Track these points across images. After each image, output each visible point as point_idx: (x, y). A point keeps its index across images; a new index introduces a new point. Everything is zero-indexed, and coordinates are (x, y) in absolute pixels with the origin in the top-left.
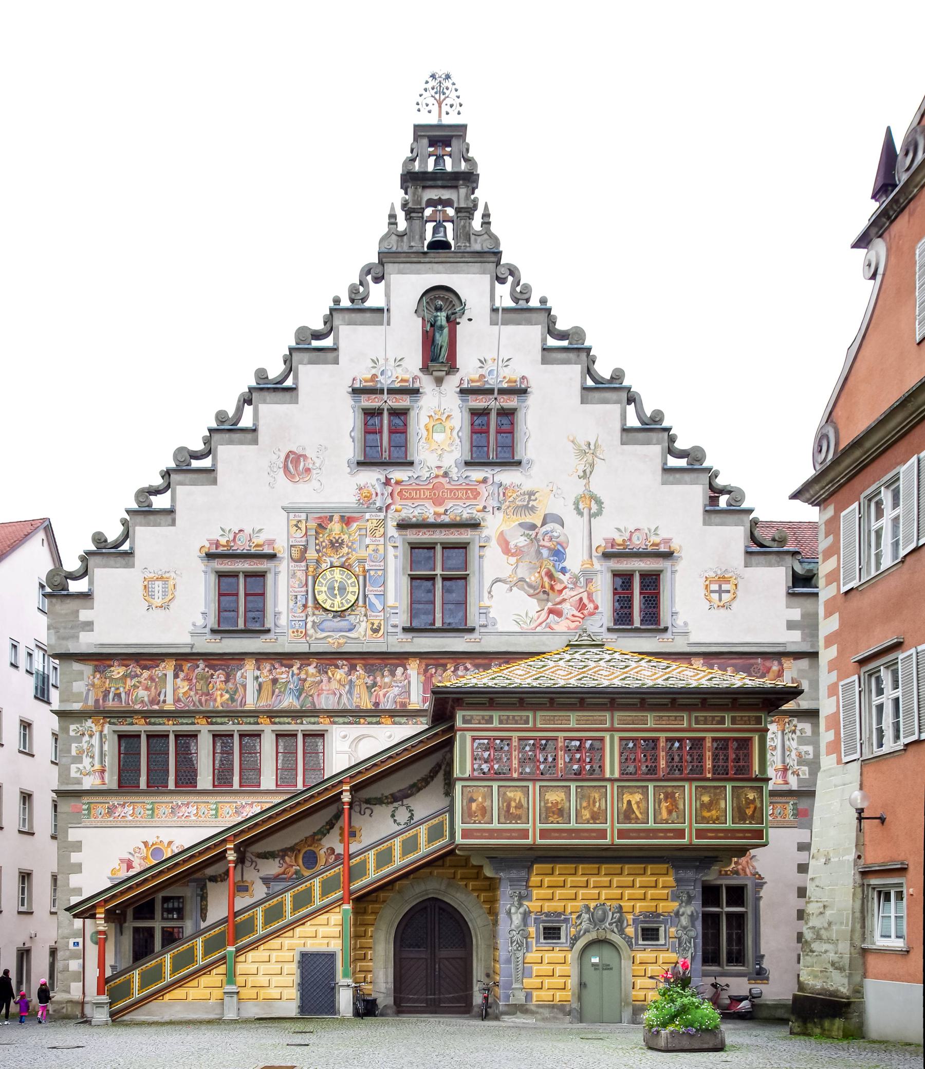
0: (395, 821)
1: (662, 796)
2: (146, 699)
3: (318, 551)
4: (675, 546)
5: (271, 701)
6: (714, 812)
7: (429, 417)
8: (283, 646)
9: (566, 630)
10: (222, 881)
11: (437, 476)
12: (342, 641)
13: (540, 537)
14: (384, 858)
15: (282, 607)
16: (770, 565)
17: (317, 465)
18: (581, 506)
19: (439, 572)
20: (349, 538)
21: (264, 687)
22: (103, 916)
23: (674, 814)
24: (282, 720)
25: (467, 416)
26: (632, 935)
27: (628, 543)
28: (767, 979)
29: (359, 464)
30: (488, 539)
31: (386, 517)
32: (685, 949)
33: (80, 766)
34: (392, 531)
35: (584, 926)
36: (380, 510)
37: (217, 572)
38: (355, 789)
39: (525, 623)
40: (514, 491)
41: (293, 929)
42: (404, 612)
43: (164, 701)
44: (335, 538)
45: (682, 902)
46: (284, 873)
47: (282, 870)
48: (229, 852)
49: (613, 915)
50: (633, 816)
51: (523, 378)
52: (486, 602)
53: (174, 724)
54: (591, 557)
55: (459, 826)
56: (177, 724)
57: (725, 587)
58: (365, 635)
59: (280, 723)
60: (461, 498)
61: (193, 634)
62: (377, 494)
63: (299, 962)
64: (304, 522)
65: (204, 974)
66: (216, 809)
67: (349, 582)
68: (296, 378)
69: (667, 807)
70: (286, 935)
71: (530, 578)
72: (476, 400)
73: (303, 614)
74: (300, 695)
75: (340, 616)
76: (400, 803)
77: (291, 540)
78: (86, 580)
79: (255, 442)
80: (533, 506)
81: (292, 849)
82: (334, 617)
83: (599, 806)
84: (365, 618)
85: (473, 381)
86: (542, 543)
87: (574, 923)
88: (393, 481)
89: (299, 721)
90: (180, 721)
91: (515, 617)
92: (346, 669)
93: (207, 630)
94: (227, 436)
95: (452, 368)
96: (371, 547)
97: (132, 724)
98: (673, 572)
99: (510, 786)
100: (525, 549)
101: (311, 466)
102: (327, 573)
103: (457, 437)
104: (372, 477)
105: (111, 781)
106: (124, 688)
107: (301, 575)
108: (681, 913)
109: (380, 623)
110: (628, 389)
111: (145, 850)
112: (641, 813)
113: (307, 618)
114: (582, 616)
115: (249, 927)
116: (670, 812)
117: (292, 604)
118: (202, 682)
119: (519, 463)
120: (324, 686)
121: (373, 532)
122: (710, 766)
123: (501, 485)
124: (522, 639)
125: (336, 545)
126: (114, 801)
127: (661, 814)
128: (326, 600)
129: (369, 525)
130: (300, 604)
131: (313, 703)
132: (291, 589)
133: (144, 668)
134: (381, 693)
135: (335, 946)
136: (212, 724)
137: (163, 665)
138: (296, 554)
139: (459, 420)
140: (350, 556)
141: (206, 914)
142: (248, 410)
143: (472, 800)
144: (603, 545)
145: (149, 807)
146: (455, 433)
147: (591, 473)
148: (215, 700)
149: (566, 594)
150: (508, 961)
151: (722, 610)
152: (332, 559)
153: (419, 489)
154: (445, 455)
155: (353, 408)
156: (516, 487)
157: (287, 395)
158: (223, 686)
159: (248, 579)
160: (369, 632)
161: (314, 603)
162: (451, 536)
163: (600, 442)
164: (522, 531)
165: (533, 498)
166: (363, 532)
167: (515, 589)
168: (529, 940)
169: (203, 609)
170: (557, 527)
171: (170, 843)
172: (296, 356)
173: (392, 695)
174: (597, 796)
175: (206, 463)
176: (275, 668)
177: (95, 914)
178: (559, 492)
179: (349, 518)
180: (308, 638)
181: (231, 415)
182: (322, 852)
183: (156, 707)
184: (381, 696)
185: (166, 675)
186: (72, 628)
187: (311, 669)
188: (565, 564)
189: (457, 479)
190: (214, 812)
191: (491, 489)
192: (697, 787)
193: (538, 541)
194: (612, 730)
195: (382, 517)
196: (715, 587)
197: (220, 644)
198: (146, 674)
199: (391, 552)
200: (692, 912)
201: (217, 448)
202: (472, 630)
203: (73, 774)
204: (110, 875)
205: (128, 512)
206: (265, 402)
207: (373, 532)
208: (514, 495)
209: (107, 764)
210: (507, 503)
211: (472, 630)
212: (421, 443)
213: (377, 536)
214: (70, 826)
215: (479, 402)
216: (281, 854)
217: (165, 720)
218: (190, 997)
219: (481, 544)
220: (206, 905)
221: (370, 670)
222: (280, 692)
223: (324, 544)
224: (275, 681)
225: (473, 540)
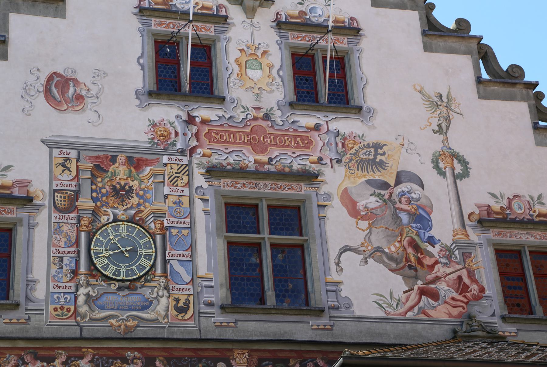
3: (95, 200)
7: (241, 51)
9: (446, 317)
11: (255, 119)
12: (131, 323)
13: (395, 197)
17: (94, 92)
18: (442, 165)
20: (140, 185)
27: (508, 212)
29: (150, 94)
30: (328, 197)
34: (199, 180)
36: (182, 152)
39: (390, 306)
40: (355, 143)
42: (221, 285)
44: (119, 184)
51: (352, 19)
54: (464, 226)
58: (166, 316)
60: (288, 146)
62: (177, 134)
64: (74, 161)
67: (142, 242)
71: (389, 248)
72: (298, 37)
75: (128, 288)
77: (54, 182)
80: (381, 161)
82: (119, 289)
84: (165, 292)
85: (292, 17)
86: (398, 205)
96: (171, 199)
100: (378, 212)
101: (84, 93)
102: (109, 228)
103: (277, 77)
109: (187, 300)
113: (77, 290)
114: (466, 300)
117: (54, 269)
121: (173, 180)
123: (338, 134)
124: (388, 327)
128: (108, 265)
129: (167, 169)
132: (53, 249)
140: (142, 207)
144: (477, 212)
146: (274, 71)
147: (448, 128)
149: (439, 270)
152: (116, 211)
154: (264, 95)
155: (141, 31)
156: (356, 139)
160: (172, 312)
161: (89, 269)
163: (453, 94)
164: (371, 190)
165: (380, 151)
166: (160, 179)
167: (371, 261)
170: (415, 187)
178: (412, 147)
179: (139, 160)
180: (79, 319)
188: (432, 233)
189: (281, 123)
191: (326, 138)
193: (394, 203)
199: (199, 206)
207: (173, 180)
208: (356, 147)
210: (348, 156)
211: (319, 312)
212: (231, 79)
213: (180, 185)
219: (321, 203)
225: (309, 197)
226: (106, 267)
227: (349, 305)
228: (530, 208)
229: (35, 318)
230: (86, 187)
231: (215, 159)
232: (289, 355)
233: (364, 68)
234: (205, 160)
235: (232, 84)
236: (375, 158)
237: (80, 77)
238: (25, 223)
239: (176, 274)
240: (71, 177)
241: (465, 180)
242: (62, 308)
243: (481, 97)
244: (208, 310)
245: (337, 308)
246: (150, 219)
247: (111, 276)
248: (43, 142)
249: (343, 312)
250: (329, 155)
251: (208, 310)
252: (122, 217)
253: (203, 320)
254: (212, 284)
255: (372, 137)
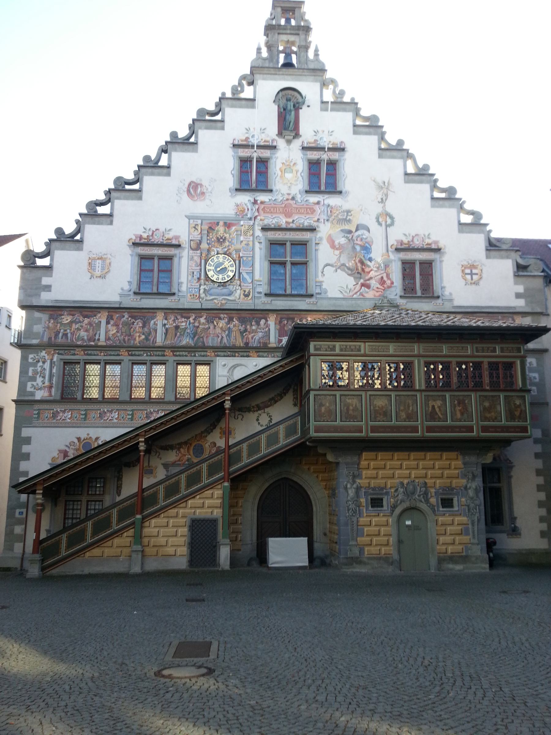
0: (259, 423)
1: (456, 402)
2: (86, 338)
3: (208, 244)
4: (441, 245)
5: (174, 340)
6: (493, 414)
7: (283, 163)
8: (184, 304)
9: (372, 297)
10: (134, 466)
11: (287, 200)
12: (223, 302)
13: (354, 238)
14: (254, 448)
15: (184, 278)
16: (502, 258)
18: (380, 220)
19: (288, 259)
21: (170, 331)
22: (41, 492)
23: (465, 415)
24: (181, 353)
25: (306, 164)
26: (435, 504)
28: (520, 534)
30: (321, 239)
31: (254, 224)
32: (472, 514)
33: (35, 383)
34: (258, 233)
35: (400, 497)
36: (250, 219)
37: (139, 255)
38: (233, 400)
39: (346, 292)
40: (337, 210)
41: (186, 501)
43: (99, 340)
45: (469, 480)
46: (179, 460)
47: (178, 458)
48: (140, 444)
49: (420, 489)
50: (437, 416)
51: (342, 142)
52: (320, 278)
53: (104, 355)
54: (388, 251)
55: (313, 424)
56: (107, 355)
57: (474, 271)
58: (240, 298)
59: (180, 356)
60: (303, 213)
61: (121, 295)
62: (248, 210)
63: (190, 526)
65: (117, 536)
66: (132, 415)
68: (197, 137)
69: (460, 410)
70: (181, 505)
73: (198, 284)
74: (194, 337)
75: (223, 286)
76: (263, 411)
78: (48, 258)
79: (169, 174)
80: (350, 219)
81: (186, 443)
82: (219, 286)
83: (412, 409)
84: (239, 287)
85: (310, 143)
86: (356, 242)
87: (393, 495)
88: (259, 202)
89: (193, 354)
90: (109, 353)
91: (340, 288)
92: (227, 320)
93: (131, 293)
94: (150, 170)
95: (297, 135)
96: (244, 243)
97: (74, 354)
98: (441, 262)
99: (348, 395)
101: (205, 191)
102: (215, 258)
104: (245, 199)
105: (55, 393)
106: (71, 330)
107: (197, 259)
108: (468, 487)
110: (407, 150)
111: (78, 444)
112: (442, 414)
115: (154, 499)
116: (462, 414)
117: (190, 277)
118: (126, 327)
119: (340, 192)
120: (211, 331)
121: (246, 233)
122: (488, 382)
124: (344, 302)
125: (221, 241)
126: (58, 408)
127: (456, 414)
129: (243, 228)
130: (195, 277)
131: (203, 342)
132: (190, 268)
133: (85, 316)
134: (250, 336)
135: (217, 513)
136: (132, 355)
137: (99, 315)
138: (193, 245)
139: (301, 166)
141: (120, 490)
142: (164, 157)
143: (321, 405)
144: (396, 244)
145: (83, 412)
147: (386, 200)
148: (135, 339)
149: (372, 274)
150: (346, 524)
151: (474, 286)
152: (218, 249)
153: (276, 208)
157: (191, 147)
158: (141, 330)
159: (161, 261)
160: (242, 296)
162: (297, 237)
164: (343, 234)
165: (349, 214)
167: (339, 270)
168: (361, 508)
169: (129, 279)
170: (365, 232)
171: (97, 439)
172: (197, 124)
173: (257, 338)
174: (410, 402)
175: (136, 187)
176: (177, 319)
177: (36, 490)
179: (229, 224)
181: (153, 159)
182: (207, 445)
183: (92, 343)
184: (250, 338)
185: (100, 322)
186: (36, 289)
187: (202, 320)
190: (130, 417)
192: (480, 396)
193: (353, 241)
194: (419, 356)
195: (252, 224)
196: (468, 271)
197: (140, 303)
198: (86, 321)
200: (476, 487)
201: (143, 177)
202: (312, 296)
203: (29, 388)
204: (50, 462)
205: (81, 215)
206: (176, 150)
209: (54, 382)
210: (333, 217)
211: (312, 296)
212: (277, 179)
214: (23, 425)
215: (314, 155)
216: (177, 446)
217: (98, 352)
218: (105, 555)
219: (317, 242)
220: (121, 484)
221: (242, 321)
222: (181, 335)
223: (213, 240)
224: (177, 327)
225: (311, 240)
226: (213, 276)
227: (326, 292)
228: (423, 241)
229: (182, 300)
230: (205, 237)
231: (266, 222)
232: (295, 316)
233: (346, 169)
234: (261, 222)
235: (277, 182)
236: (347, 217)
237: (204, 183)
238: (178, 256)
239: (244, 279)
240: (198, 233)
241: (392, 228)
242: (193, 295)
243: (406, 182)
244: (259, 295)
245: (320, 294)
246: (234, 253)
247: (215, 280)
248: (186, 216)
249: (323, 295)
250: (323, 217)
251: (259, 295)
252: (220, 252)
253: (256, 300)
254: (261, 283)
255: (346, 207)
